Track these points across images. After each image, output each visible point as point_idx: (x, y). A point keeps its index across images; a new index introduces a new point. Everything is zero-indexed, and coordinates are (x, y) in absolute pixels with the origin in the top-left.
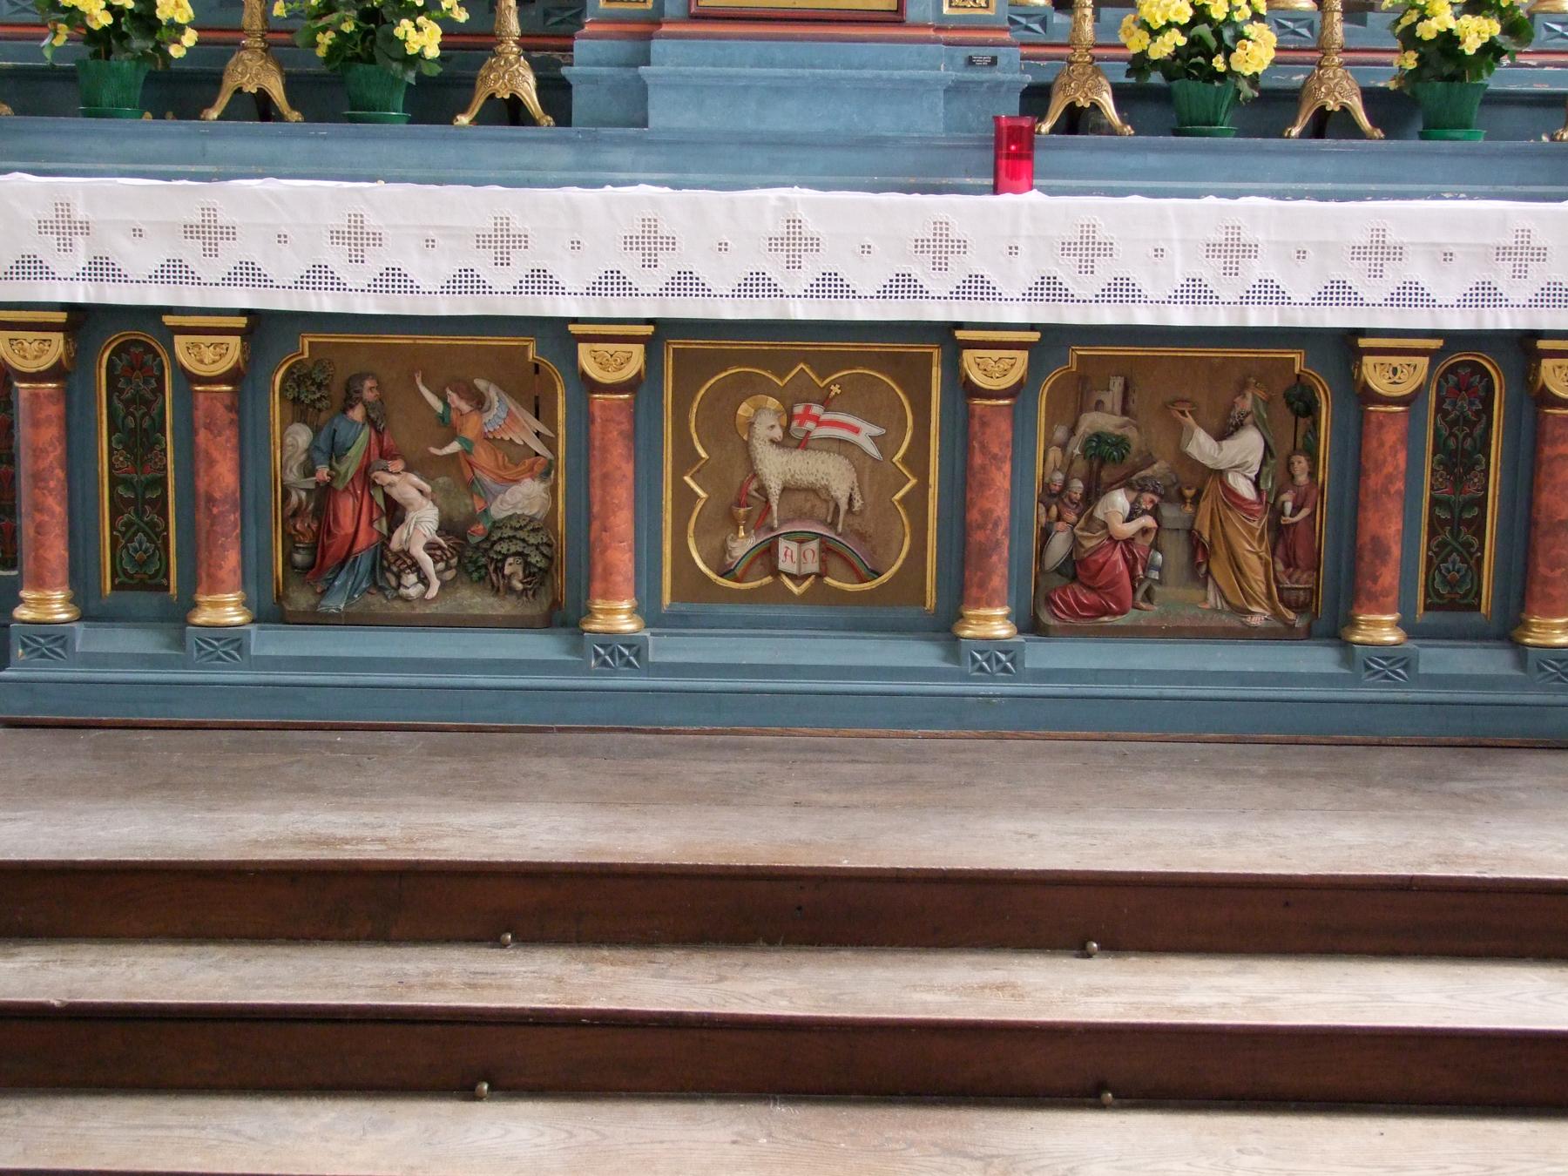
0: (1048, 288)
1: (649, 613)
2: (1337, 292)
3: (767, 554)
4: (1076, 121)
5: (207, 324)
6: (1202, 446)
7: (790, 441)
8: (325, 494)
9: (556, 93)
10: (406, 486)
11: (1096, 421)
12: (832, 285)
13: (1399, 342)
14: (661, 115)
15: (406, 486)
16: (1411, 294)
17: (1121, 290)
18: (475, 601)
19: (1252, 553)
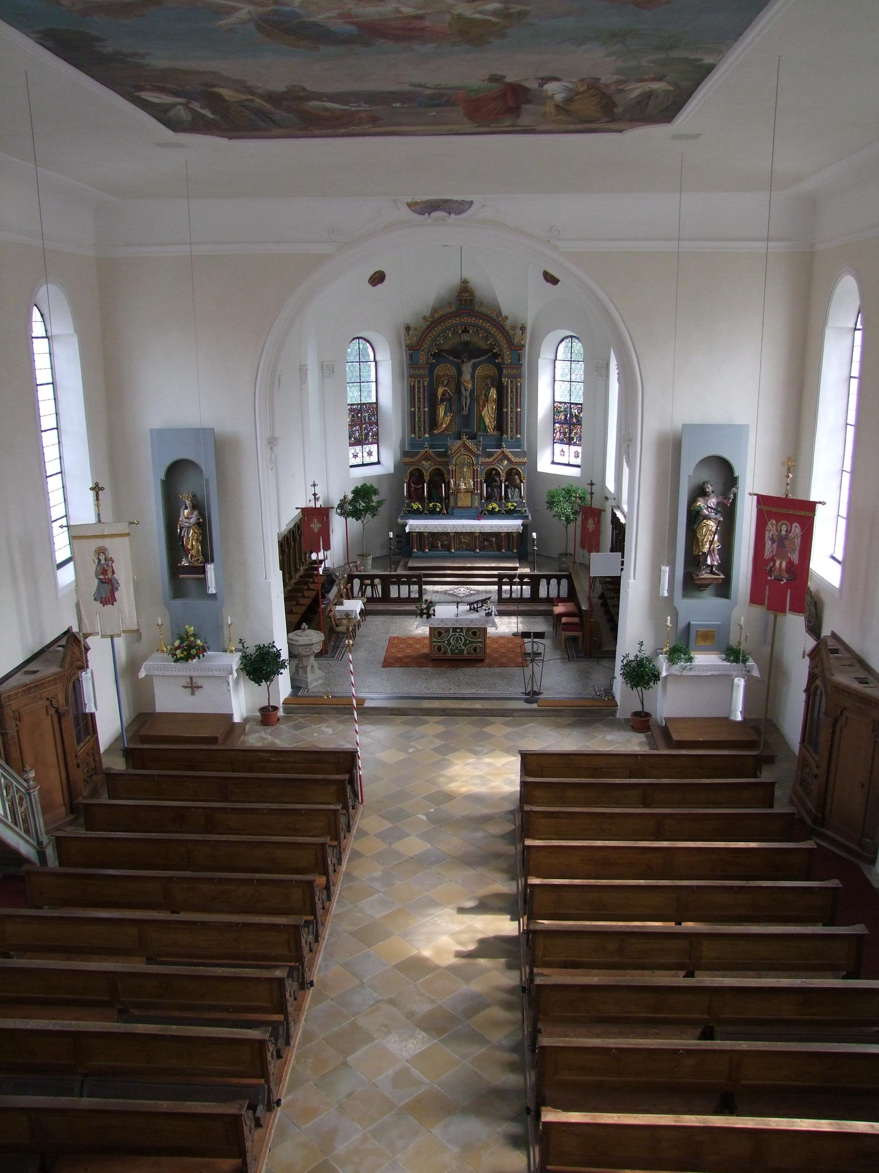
0: (480, 530)
1: (455, 550)
2: (498, 530)
3: (462, 546)
4: (486, 514)
5: (426, 532)
6: (491, 539)
7: (464, 539)
8: (433, 543)
9: (447, 513)
10: (439, 542)
11: (485, 537)
12: (466, 529)
13: (503, 532)
14: (455, 514)
15: (439, 542)
16: (503, 530)
17: (485, 530)
18: (443, 549)
19: (495, 546)
